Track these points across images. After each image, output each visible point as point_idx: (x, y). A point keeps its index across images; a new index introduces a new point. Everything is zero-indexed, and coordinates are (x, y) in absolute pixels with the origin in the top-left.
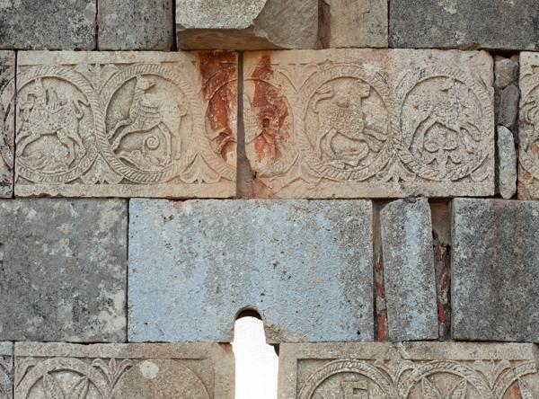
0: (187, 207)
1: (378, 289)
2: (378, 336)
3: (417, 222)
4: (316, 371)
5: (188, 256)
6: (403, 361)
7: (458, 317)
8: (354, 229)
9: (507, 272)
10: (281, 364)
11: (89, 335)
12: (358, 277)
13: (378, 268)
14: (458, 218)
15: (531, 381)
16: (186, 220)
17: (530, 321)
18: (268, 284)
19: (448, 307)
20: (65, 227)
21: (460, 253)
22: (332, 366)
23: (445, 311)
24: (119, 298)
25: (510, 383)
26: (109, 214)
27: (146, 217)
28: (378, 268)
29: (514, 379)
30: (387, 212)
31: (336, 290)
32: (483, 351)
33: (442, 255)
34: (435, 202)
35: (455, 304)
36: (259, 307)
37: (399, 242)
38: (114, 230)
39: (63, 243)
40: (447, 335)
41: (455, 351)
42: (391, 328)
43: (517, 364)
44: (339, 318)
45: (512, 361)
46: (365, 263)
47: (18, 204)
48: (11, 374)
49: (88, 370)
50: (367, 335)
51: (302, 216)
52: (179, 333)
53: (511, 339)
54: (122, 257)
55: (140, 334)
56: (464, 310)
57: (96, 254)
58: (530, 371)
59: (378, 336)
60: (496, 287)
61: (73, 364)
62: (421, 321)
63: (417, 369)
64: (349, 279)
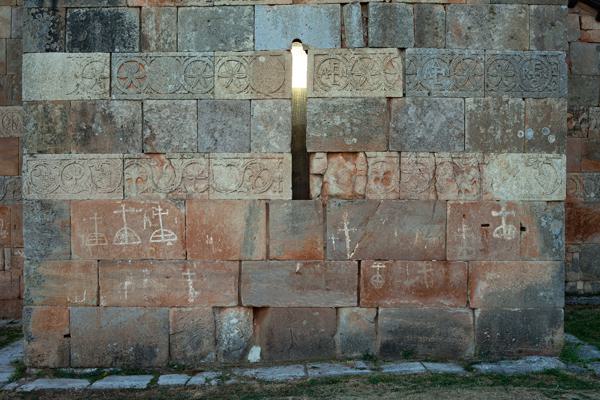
0: (275, 7)
1: (342, 32)
2: (342, 47)
3: (356, 11)
4: (321, 58)
5: (275, 23)
6: (351, 54)
7: (371, 40)
8: (333, 14)
9: (388, 25)
10: (308, 59)
11: (241, 48)
12: (335, 28)
13: (342, 25)
14: (371, 9)
15: (396, 60)
16: (275, 11)
18: (304, 31)
19: (367, 37)
20: (232, 15)
21: (371, 20)
22: (326, 57)
23: (366, 38)
24: (251, 37)
26: (248, 10)
27: (260, 12)
28: (342, 25)
30: (345, 7)
31: (327, 32)
32: (379, 50)
33: (365, 21)
34: (362, 4)
35: (370, 36)
36: (301, 38)
37: (350, 17)
38: (249, 15)
39: (231, 20)
40: (367, 45)
41: (369, 51)
42: (347, 44)
44: (329, 42)
46: (338, 24)
47: (215, 8)
48: (213, 62)
49: (241, 60)
50: (339, 46)
51: (316, 9)
52: (272, 48)
54: (252, 24)
55: (259, 48)
56: (373, 38)
57: (244, 23)
59: (342, 47)
60: (384, 30)
61: (234, 58)
62: (358, 41)
63: (356, 57)
64: (333, 29)
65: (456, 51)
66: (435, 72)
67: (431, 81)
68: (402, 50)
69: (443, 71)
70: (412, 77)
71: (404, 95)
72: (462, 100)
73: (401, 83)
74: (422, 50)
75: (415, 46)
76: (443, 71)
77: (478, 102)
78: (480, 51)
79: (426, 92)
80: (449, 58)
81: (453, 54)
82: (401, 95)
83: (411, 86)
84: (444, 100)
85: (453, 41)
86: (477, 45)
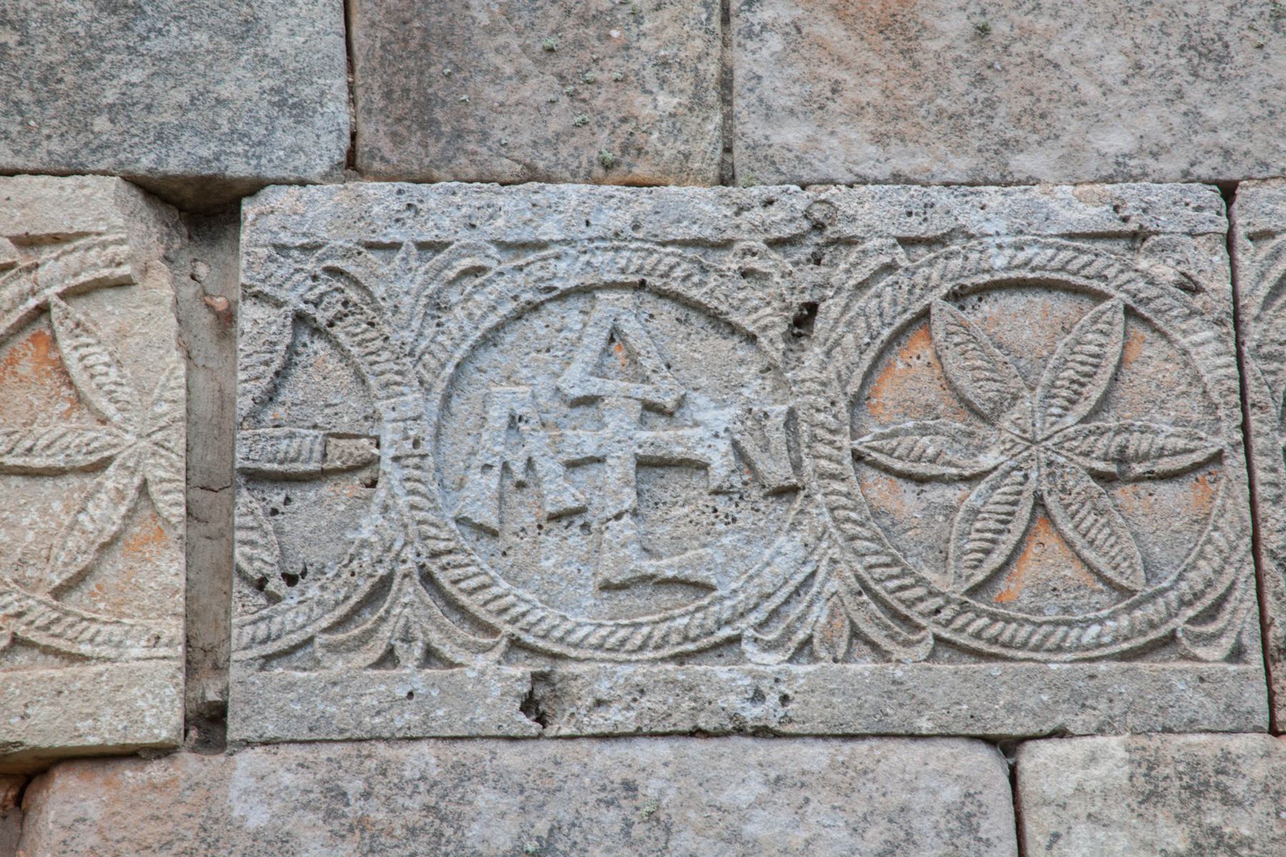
17: (110, 96)
25: (13, 318)
29: (32, 302)
43: (47, 254)
45: (27, 242)
53: (19, 162)
58: (105, 272)
65: (873, 214)
66: (619, 434)
67: (558, 553)
68: (201, 210)
69: (707, 432)
70: (310, 511)
71: (209, 725)
72: (985, 757)
73: (170, 568)
74: (444, 208)
75: (352, 164)
76: (707, 432)
77: (1202, 785)
78: (1173, 205)
79: (494, 681)
80: (788, 277)
81: (822, 238)
82: (160, 718)
83: (294, 614)
84: (741, 773)
85: (814, 107)
86: (1116, 141)
